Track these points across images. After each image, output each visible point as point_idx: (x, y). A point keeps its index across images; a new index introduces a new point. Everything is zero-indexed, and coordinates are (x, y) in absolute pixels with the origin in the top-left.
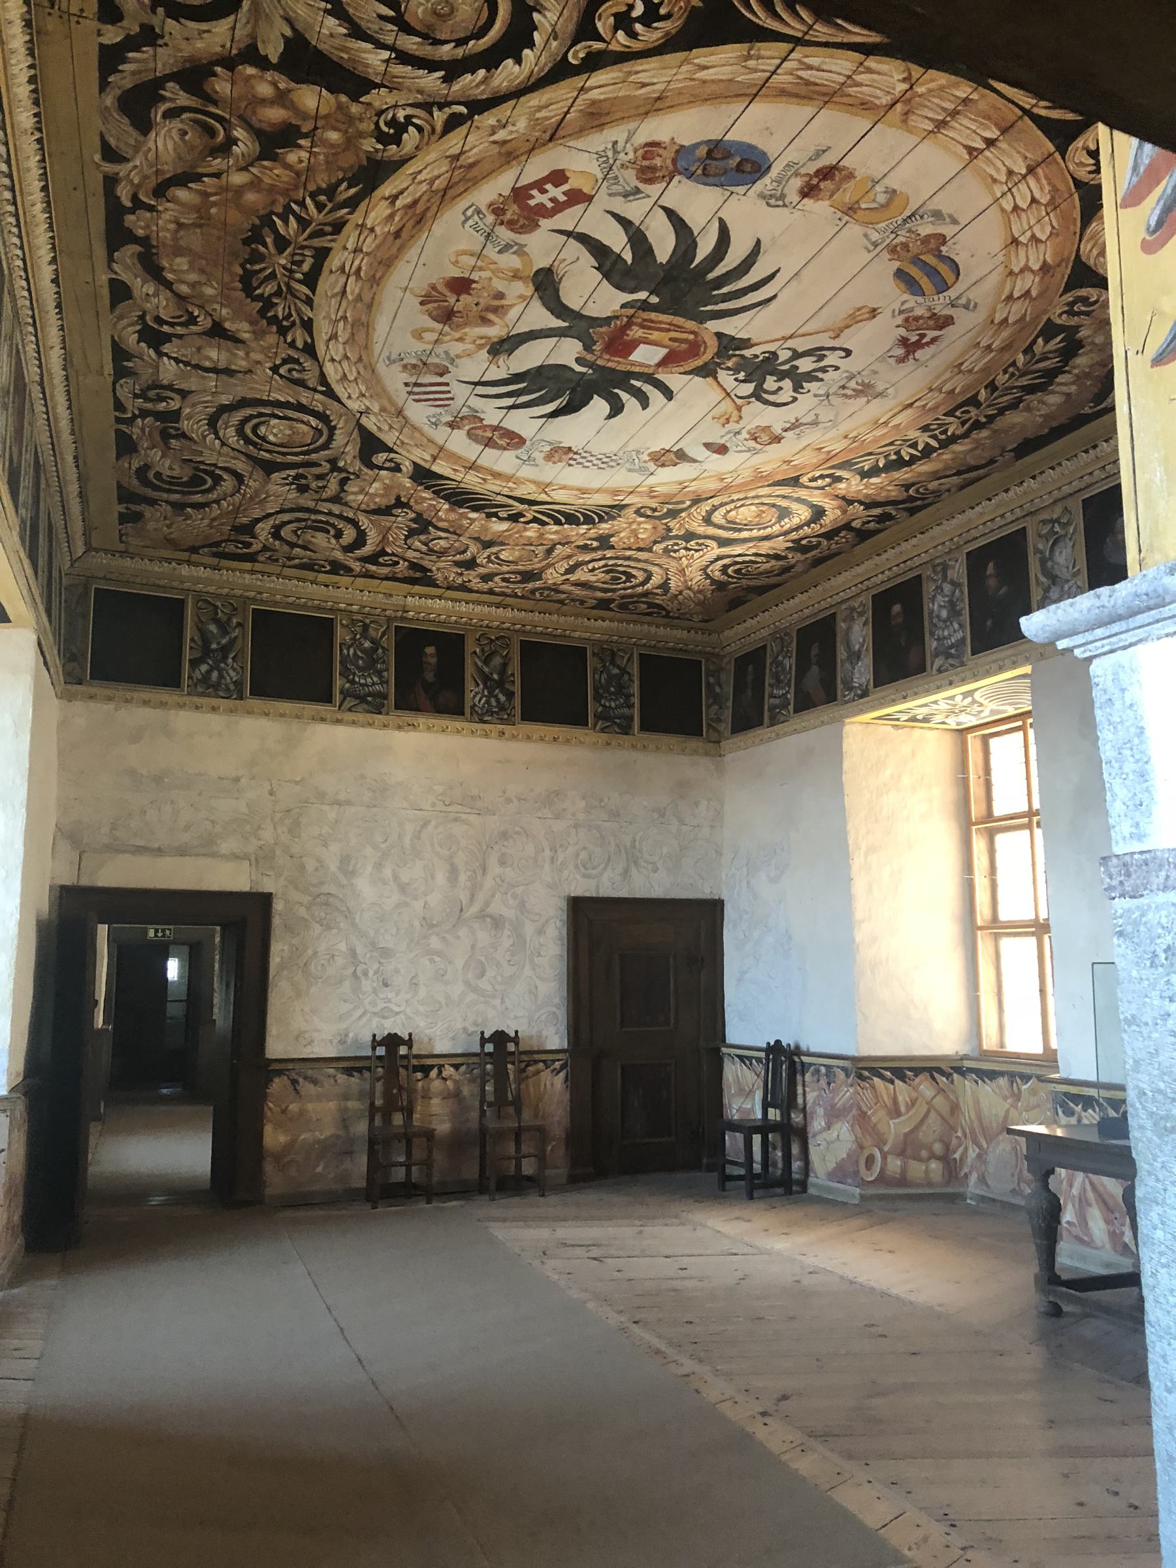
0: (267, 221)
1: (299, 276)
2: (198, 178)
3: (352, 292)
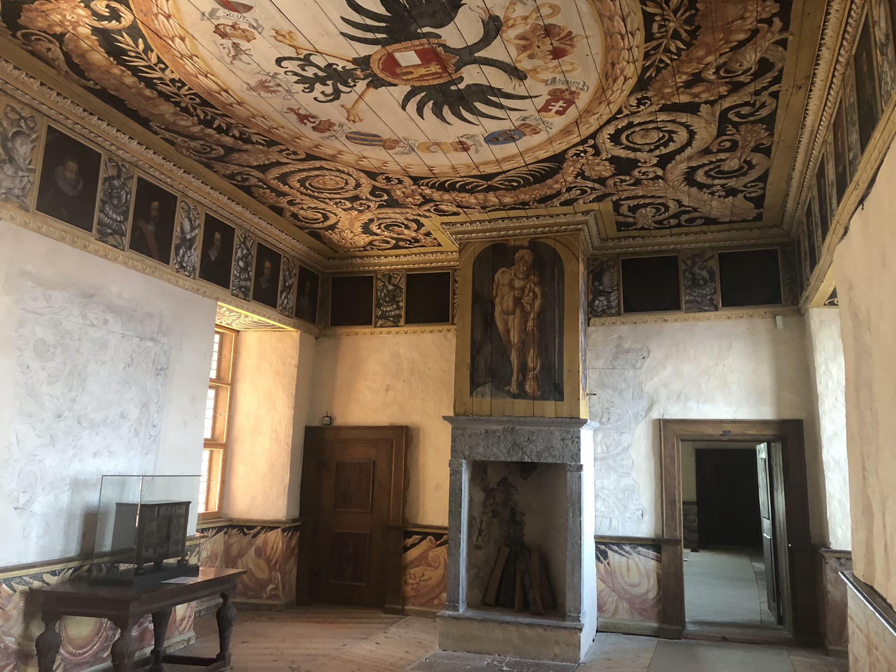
0: (688, 45)
1: (658, 18)
2: (732, 49)
3: (618, 23)
